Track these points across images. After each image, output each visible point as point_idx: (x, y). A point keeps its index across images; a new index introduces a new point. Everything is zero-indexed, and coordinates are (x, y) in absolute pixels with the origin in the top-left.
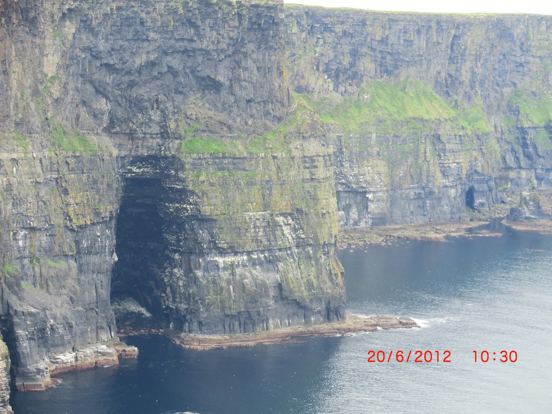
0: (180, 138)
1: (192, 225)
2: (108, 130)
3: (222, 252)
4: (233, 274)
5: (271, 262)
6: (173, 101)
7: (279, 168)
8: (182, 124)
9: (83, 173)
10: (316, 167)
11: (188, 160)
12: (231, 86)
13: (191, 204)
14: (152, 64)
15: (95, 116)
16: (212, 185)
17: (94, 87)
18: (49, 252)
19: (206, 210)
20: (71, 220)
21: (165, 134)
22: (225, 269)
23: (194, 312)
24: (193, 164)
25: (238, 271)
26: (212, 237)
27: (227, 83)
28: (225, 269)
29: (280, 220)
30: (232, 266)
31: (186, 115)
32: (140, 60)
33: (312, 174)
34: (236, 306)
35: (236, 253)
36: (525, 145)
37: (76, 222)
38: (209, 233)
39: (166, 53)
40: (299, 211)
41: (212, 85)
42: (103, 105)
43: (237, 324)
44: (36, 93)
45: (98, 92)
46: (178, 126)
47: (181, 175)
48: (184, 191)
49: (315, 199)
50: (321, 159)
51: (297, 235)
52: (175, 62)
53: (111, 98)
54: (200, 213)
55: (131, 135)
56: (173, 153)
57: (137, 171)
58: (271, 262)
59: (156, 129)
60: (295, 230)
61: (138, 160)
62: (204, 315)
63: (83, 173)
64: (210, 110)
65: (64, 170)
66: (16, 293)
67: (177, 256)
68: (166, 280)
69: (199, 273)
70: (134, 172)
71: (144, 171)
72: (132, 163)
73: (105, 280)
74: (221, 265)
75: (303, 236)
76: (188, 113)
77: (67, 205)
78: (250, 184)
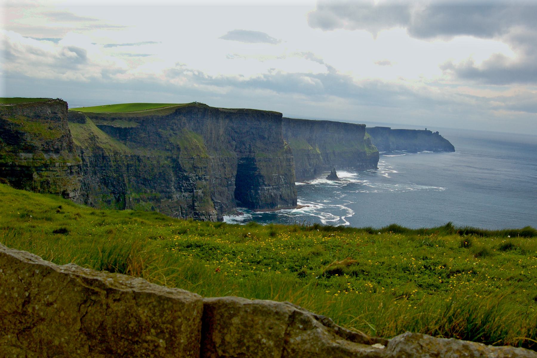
0: (254, 153)
2: (235, 150)
3: (266, 186)
5: (278, 189)
7: (281, 162)
11: (257, 159)
14: (247, 132)
18: (220, 185)
19: (262, 173)
21: (250, 152)
23: (258, 203)
25: (270, 191)
29: (281, 176)
32: (245, 131)
34: (269, 201)
35: (269, 186)
36: (327, 158)
37: (228, 176)
39: (251, 128)
40: (286, 174)
41: (263, 138)
42: (234, 143)
44: (218, 139)
47: (255, 163)
48: (256, 168)
49: (290, 171)
52: (254, 131)
55: (241, 152)
58: (278, 189)
59: (248, 150)
60: (284, 179)
61: (242, 159)
62: (260, 204)
65: (225, 161)
66: (214, 196)
69: (259, 192)
72: (241, 160)
73: (233, 193)
78: (273, 166)
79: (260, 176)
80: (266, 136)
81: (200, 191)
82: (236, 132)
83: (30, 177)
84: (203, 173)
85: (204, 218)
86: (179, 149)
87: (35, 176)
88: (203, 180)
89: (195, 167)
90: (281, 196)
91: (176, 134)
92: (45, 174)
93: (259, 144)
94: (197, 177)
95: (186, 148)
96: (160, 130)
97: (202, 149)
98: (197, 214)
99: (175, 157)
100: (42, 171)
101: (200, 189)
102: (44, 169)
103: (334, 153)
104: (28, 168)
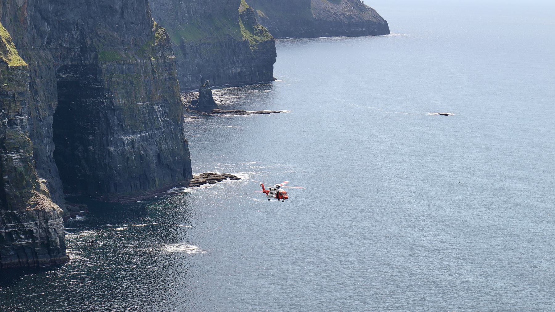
1: (106, 114)
4: (133, 147)
6: (88, 23)
8: (95, 40)
9: (42, 78)
10: (172, 70)
12: (122, 14)
13: (106, 98)
15: (41, 36)
16: (118, 83)
17: (41, 14)
20: (40, 114)
22: (128, 144)
24: (107, 70)
26: (120, 122)
27: (120, 11)
28: (128, 144)
29: (156, 107)
30: (133, 142)
31: (97, 33)
33: (170, 75)
35: (134, 133)
37: (43, 114)
38: (118, 119)
42: (47, 28)
43: (138, 182)
45: (43, 18)
46: (92, 42)
50: (174, 64)
51: (164, 119)
53: (51, 22)
54: (113, 105)
56: (91, 62)
57: (64, 76)
60: (163, 115)
61: (64, 68)
63: (42, 78)
64: (110, 30)
67: (91, 137)
68: (80, 155)
70: (61, 77)
71: (68, 76)
74: (126, 142)
75: (168, 119)
76: (99, 33)
77: (37, 101)
79: (113, 109)
80: (117, 7)
84: (19, 108)
85: (33, 227)
88: (19, 128)
90: (159, 156)
94: (6, 121)
97: (8, 46)
98: (16, 218)
101: (17, 150)
103: (183, 47)
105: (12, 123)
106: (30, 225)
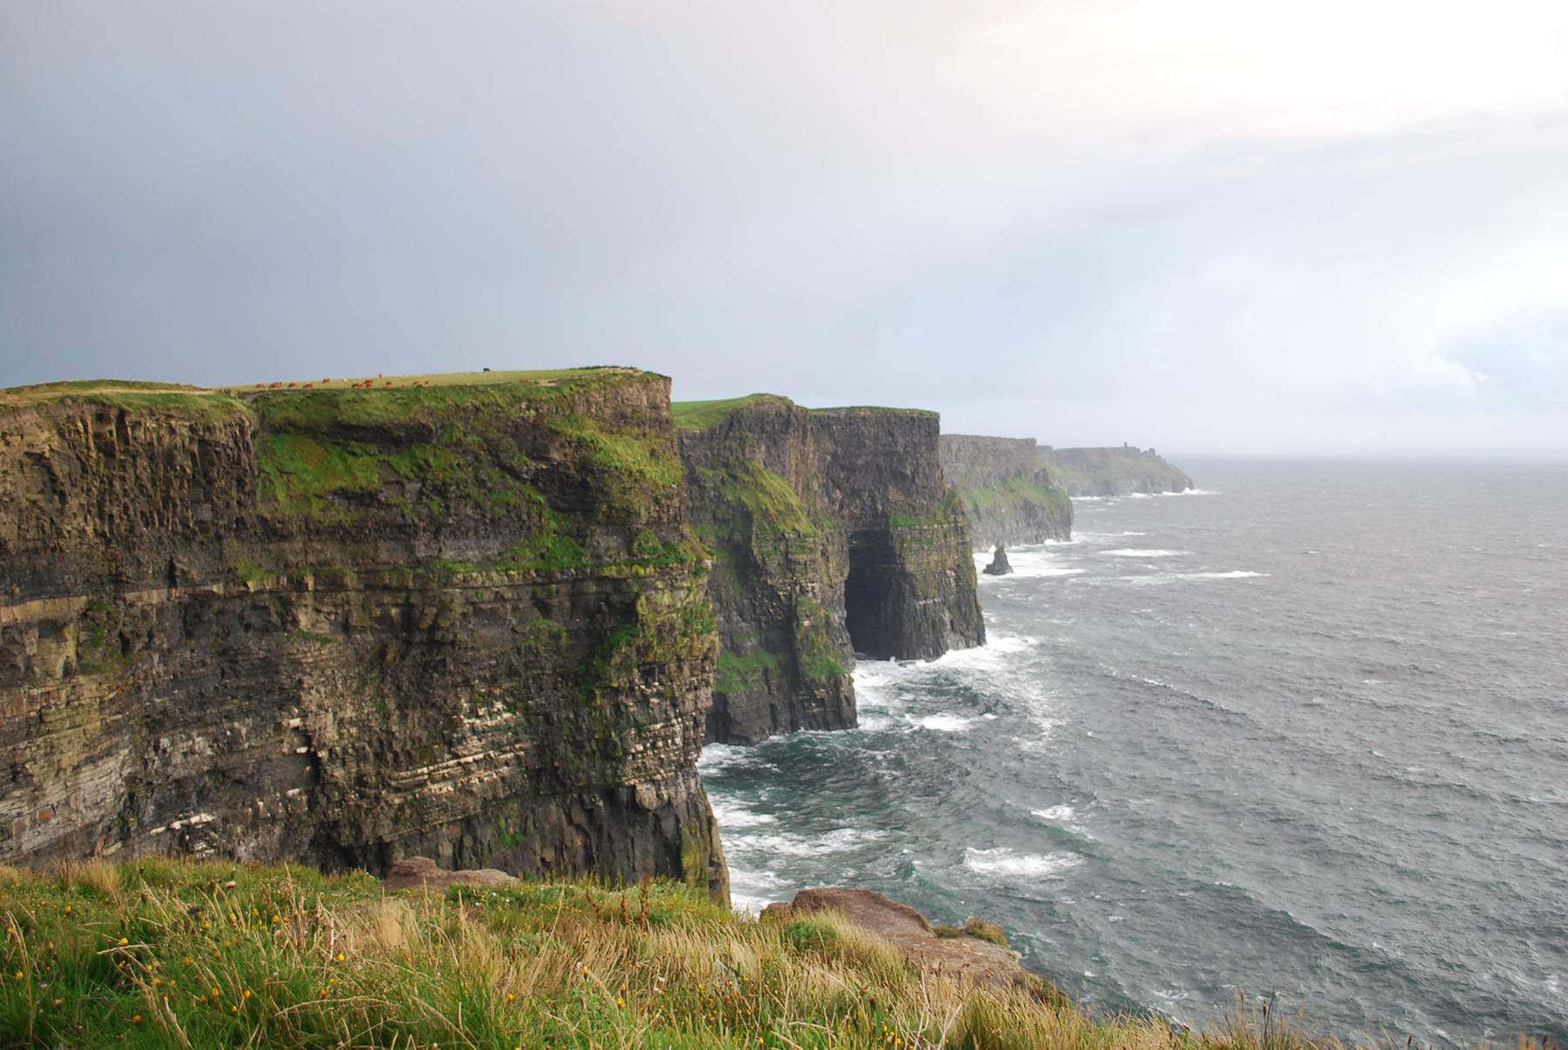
19: (910, 568)
21: (875, 515)
42: (838, 495)
61: (854, 536)
79: (905, 575)
81: (806, 623)
82: (843, 467)
83: (628, 613)
86: (748, 516)
87: (642, 608)
89: (789, 561)
91: (734, 477)
92: (666, 599)
93: (894, 495)
95: (765, 514)
96: (699, 469)
99: (737, 537)
100: (656, 589)
102: (660, 584)
104: (617, 583)
105: (803, 591)
106: (821, 693)
